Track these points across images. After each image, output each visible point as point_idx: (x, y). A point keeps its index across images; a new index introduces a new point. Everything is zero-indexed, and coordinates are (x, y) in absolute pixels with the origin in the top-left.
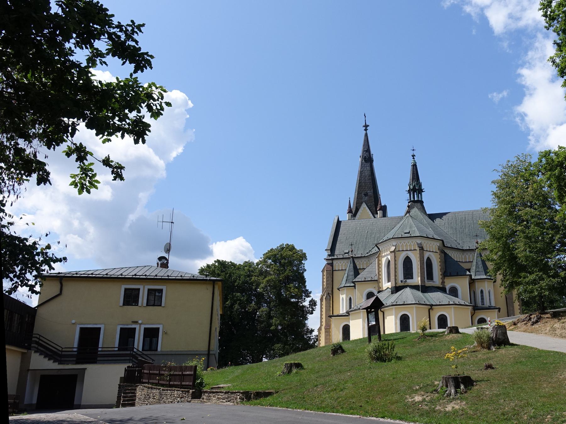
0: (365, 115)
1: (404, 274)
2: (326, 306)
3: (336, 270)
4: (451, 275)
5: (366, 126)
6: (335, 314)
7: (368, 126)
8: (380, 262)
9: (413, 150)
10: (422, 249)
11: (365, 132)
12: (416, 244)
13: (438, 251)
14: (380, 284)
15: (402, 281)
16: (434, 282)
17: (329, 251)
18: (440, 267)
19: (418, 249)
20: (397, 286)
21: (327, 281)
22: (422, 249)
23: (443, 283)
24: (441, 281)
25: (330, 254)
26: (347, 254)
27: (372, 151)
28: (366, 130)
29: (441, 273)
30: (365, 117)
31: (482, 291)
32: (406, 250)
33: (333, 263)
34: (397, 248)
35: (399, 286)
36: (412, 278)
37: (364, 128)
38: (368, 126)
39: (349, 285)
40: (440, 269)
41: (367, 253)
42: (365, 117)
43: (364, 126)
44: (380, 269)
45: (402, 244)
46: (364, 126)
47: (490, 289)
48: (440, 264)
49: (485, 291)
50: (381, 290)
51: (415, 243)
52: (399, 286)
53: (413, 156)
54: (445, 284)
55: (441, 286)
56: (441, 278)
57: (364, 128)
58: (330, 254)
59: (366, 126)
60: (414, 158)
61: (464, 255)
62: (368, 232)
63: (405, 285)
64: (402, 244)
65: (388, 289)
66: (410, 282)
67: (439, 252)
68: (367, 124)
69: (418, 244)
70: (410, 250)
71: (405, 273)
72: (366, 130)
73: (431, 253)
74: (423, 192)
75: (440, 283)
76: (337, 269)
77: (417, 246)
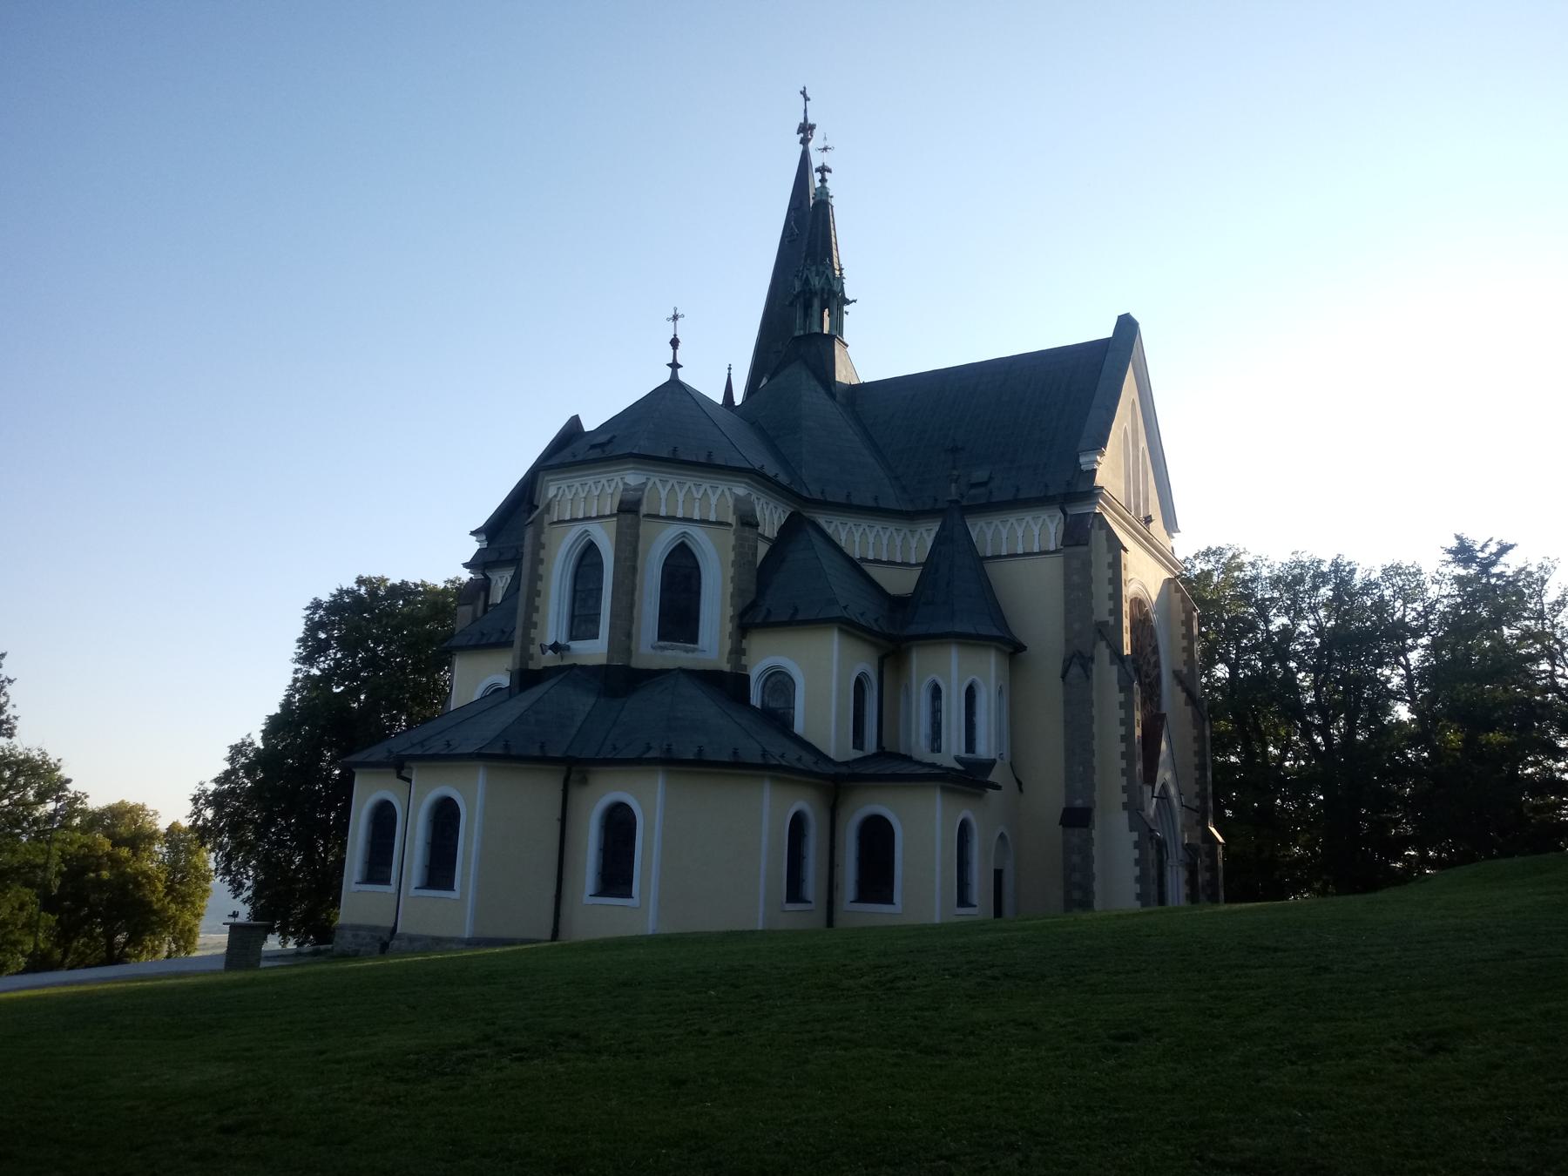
4: (771, 624)
7: (812, 127)
8: (541, 570)
18: (730, 588)
20: (532, 666)
23: (738, 652)
24: (728, 645)
28: (805, 142)
29: (730, 611)
30: (807, 99)
31: (936, 692)
32: (574, 520)
35: (546, 669)
38: (812, 127)
40: (732, 596)
42: (807, 99)
45: (574, 490)
47: (979, 680)
48: (731, 572)
61: (917, 536)
64: (574, 490)
67: (734, 524)
68: (810, 121)
70: (599, 517)
72: (805, 142)
74: (848, 302)
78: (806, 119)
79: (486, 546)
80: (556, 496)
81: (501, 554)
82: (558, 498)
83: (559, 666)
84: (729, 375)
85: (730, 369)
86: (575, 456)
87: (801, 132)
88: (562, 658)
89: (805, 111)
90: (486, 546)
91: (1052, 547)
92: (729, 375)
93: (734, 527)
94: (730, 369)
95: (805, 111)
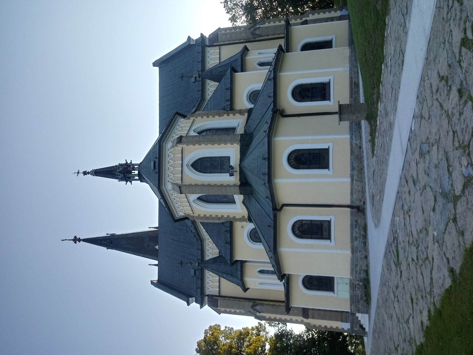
0: (63, 240)
1: (221, 173)
2: (272, 313)
3: (219, 291)
4: (231, 100)
5: (76, 240)
6: (283, 298)
7: (75, 237)
9: (78, 173)
10: (180, 140)
11: (81, 242)
12: (173, 149)
13: (192, 119)
14: (237, 217)
15: (231, 175)
16: (238, 126)
17: (191, 299)
18: (217, 117)
19: (180, 147)
20: (239, 183)
21: (232, 307)
22: (180, 140)
23: (241, 112)
24: (238, 115)
25: (194, 299)
26: (197, 272)
27: (102, 234)
28: (79, 240)
30: (66, 240)
33: (208, 295)
34: (176, 182)
35: (240, 180)
36: (228, 158)
37: (77, 242)
38: (75, 237)
39: (239, 273)
40: (220, 116)
41: (197, 241)
42: (66, 240)
43: (75, 243)
44: (214, 216)
46: (75, 243)
49: (260, 58)
50: (246, 217)
51: (170, 151)
52: (240, 180)
53: (85, 173)
54: (244, 108)
55: (246, 114)
56: (234, 115)
57: (77, 242)
58: (194, 299)
59: (76, 240)
60: (88, 173)
62: (172, 240)
63: (238, 170)
65: (245, 203)
66: (235, 161)
68: (73, 238)
69: (172, 147)
70: (182, 160)
71: (219, 171)
72: (79, 240)
73: (193, 128)
74: (131, 163)
75: (241, 116)
76: (218, 289)
77: (176, 148)
78: (72, 240)
79: (195, 298)
80: (171, 183)
81: (198, 279)
82: (172, 181)
83: (239, 173)
84: (152, 265)
85: (150, 265)
86: (157, 173)
87: (76, 242)
88: (237, 172)
89: (69, 240)
90: (195, 298)
91: (218, 51)
92: (152, 265)
93: (194, 118)
94: (150, 265)
95: (69, 240)
